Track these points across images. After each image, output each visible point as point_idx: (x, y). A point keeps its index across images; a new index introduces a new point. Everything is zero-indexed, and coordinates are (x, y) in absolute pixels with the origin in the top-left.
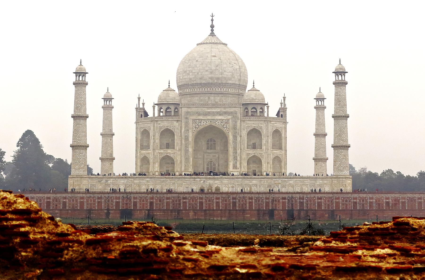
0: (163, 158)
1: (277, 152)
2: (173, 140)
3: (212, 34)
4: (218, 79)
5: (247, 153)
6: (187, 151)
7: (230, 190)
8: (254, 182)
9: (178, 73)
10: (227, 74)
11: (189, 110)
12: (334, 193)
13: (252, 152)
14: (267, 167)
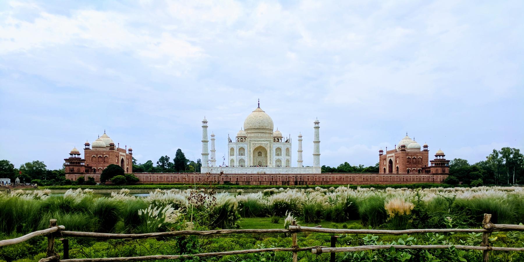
0: (240, 160)
1: (287, 157)
2: (244, 152)
3: (259, 107)
5: (275, 158)
6: (250, 157)
8: (280, 170)
9: (245, 124)
10: (266, 124)
13: (277, 157)
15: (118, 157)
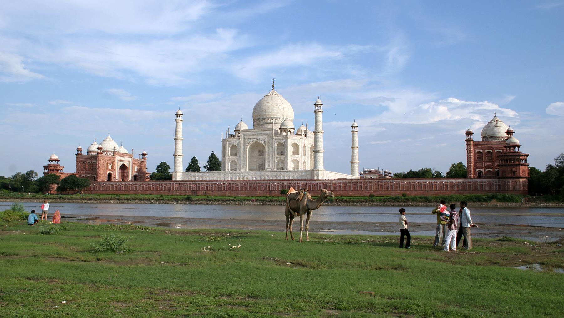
1: (296, 157)
4: (269, 115)
7: (254, 179)
11: (245, 133)
12: (307, 180)
14: (290, 166)
15: (113, 163)
